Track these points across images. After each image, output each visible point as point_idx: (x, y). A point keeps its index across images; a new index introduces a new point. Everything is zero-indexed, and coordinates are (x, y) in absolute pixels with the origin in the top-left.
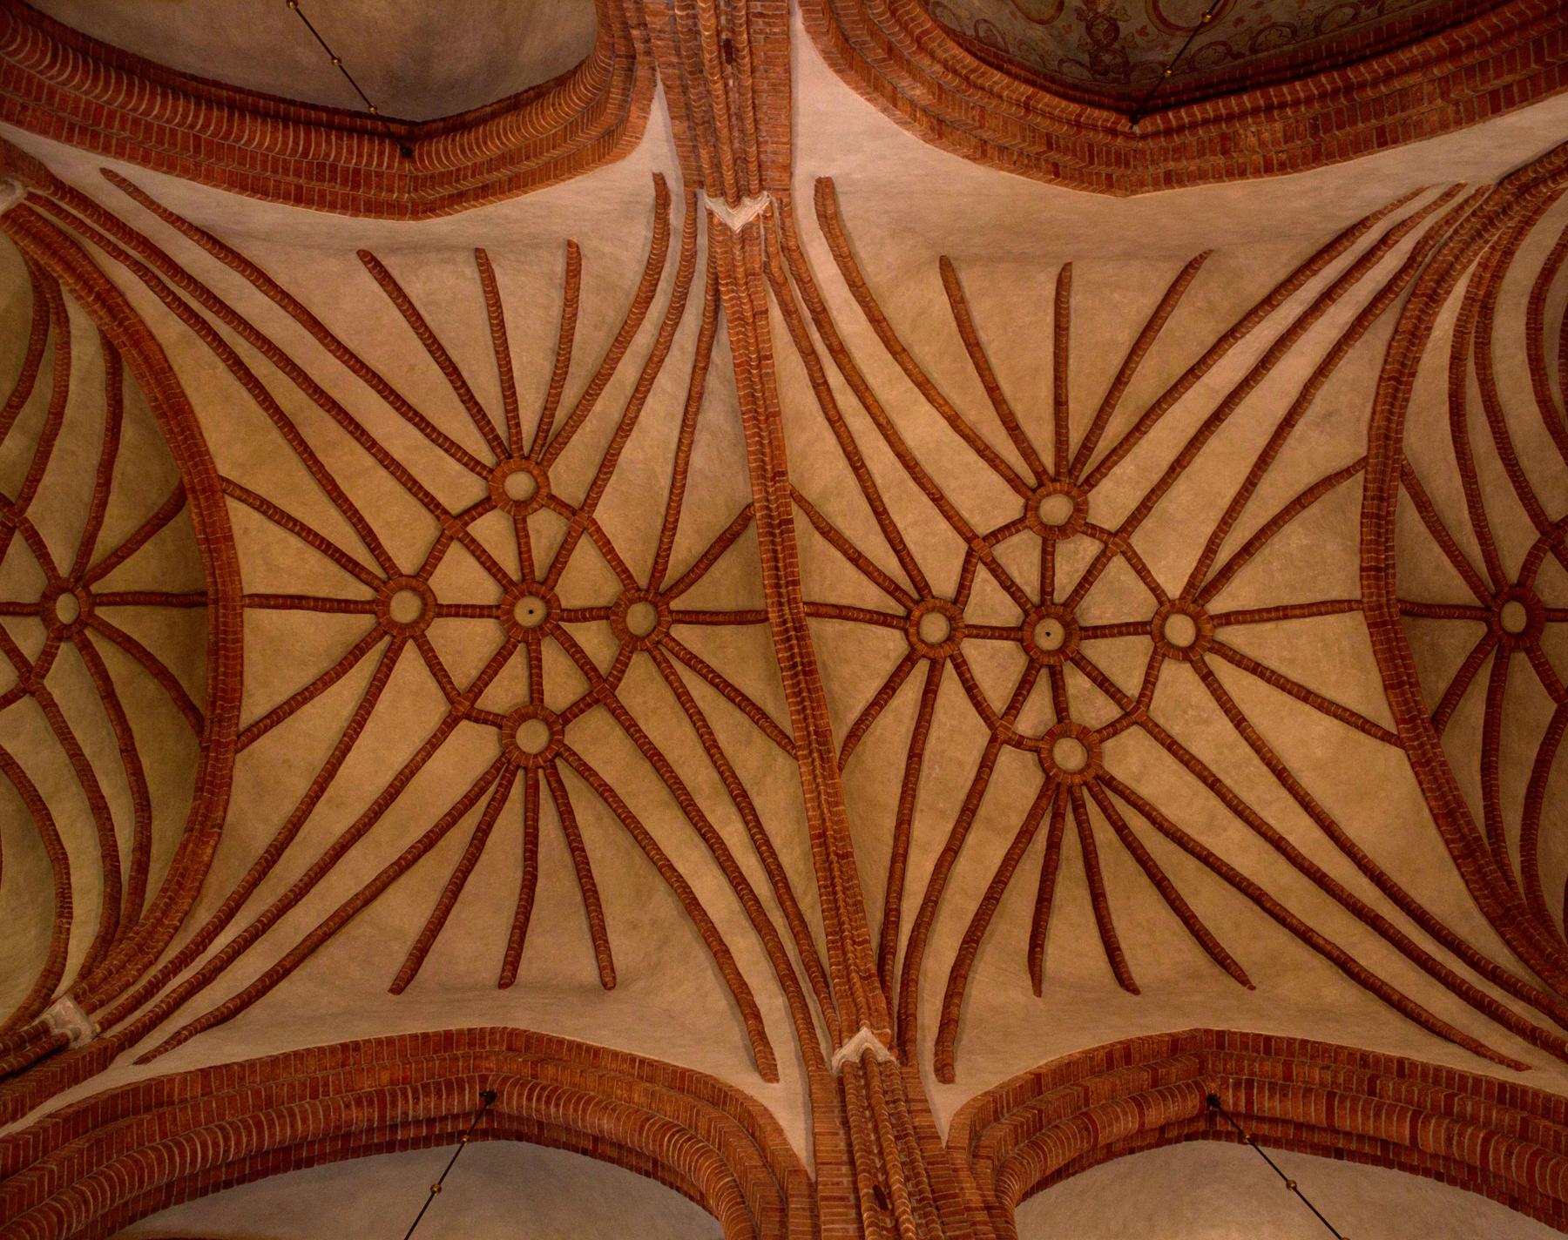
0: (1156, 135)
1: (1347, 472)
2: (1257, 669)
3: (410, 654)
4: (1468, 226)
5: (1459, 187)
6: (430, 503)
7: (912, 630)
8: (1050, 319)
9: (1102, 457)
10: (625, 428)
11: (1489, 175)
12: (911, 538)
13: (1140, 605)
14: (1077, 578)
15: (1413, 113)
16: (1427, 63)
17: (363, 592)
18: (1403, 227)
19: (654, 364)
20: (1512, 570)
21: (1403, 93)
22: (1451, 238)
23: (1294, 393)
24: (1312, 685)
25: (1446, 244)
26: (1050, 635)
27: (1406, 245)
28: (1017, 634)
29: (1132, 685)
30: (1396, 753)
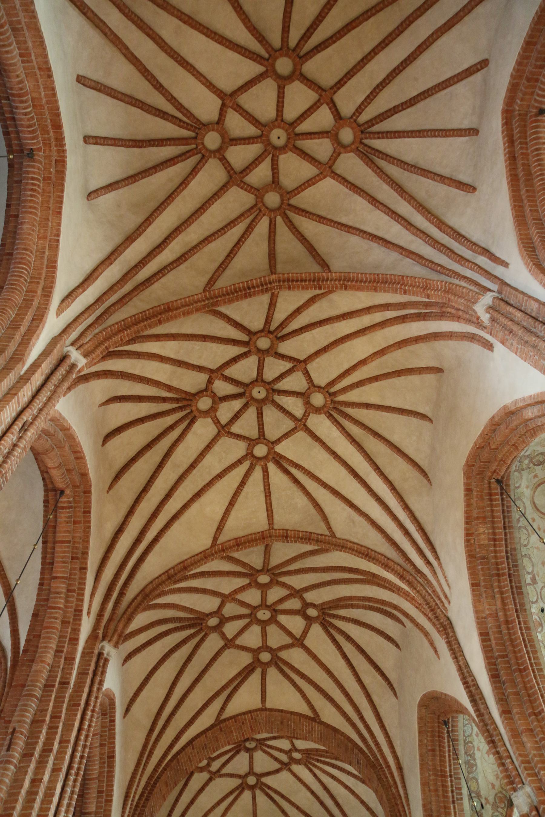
0: (490, 488)
1: (329, 528)
2: (243, 483)
3: (258, 69)
4: (432, 600)
5: (449, 602)
6: (340, 83)
7: (263, 334)
8: (407, 407)
9: (341, 422)
10: (374, 201)
11: (453, 614)
12: (307, 336)
13: (272, 433)
14: (285, 406)
15: (484, 599)
16: (505, 610)
17: (294, 39)
18: (434, 573)
19: (407, 224)
20: (284, 579)
21: (494, 597)
22: (427, 592)
23: (364, 509)
24: (236, 506)
25: (425, 589)
26: (259, 393)
27: (425, 570)
28: (259, 380)
29: (235, 429)
30: (208, 543)
